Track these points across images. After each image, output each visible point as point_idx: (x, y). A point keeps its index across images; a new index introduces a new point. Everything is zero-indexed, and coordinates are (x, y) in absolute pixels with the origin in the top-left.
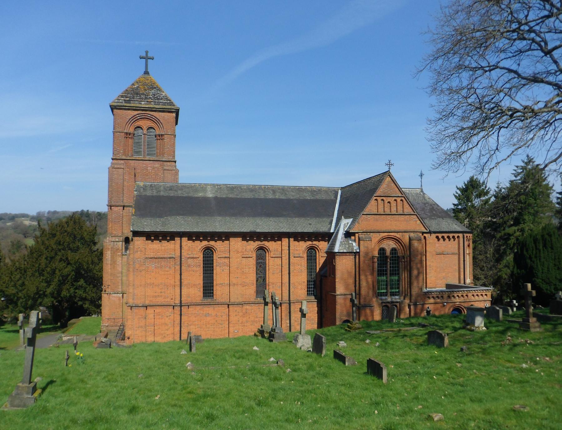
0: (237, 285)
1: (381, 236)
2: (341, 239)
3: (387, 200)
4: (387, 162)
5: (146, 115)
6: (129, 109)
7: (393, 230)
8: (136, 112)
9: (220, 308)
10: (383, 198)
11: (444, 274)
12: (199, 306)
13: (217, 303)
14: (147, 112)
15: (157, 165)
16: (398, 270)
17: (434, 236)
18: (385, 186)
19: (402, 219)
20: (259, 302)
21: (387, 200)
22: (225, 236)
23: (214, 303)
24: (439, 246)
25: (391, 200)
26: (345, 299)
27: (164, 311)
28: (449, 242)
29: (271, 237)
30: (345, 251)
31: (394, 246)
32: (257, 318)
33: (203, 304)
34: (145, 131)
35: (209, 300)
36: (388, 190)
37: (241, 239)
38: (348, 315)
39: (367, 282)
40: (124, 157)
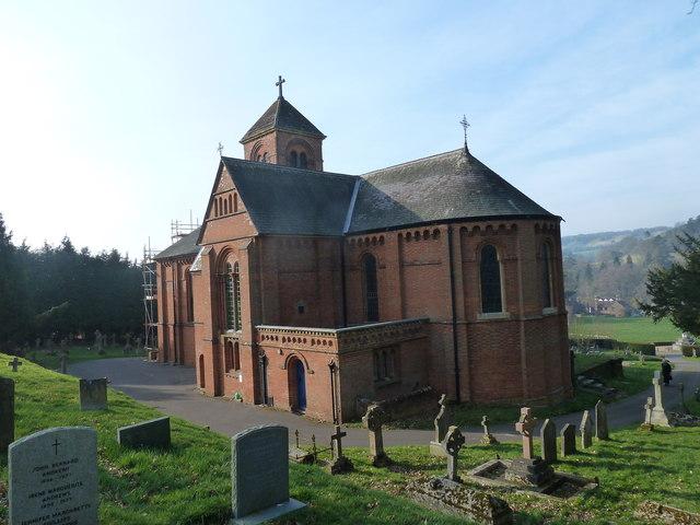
17: (396, 233)
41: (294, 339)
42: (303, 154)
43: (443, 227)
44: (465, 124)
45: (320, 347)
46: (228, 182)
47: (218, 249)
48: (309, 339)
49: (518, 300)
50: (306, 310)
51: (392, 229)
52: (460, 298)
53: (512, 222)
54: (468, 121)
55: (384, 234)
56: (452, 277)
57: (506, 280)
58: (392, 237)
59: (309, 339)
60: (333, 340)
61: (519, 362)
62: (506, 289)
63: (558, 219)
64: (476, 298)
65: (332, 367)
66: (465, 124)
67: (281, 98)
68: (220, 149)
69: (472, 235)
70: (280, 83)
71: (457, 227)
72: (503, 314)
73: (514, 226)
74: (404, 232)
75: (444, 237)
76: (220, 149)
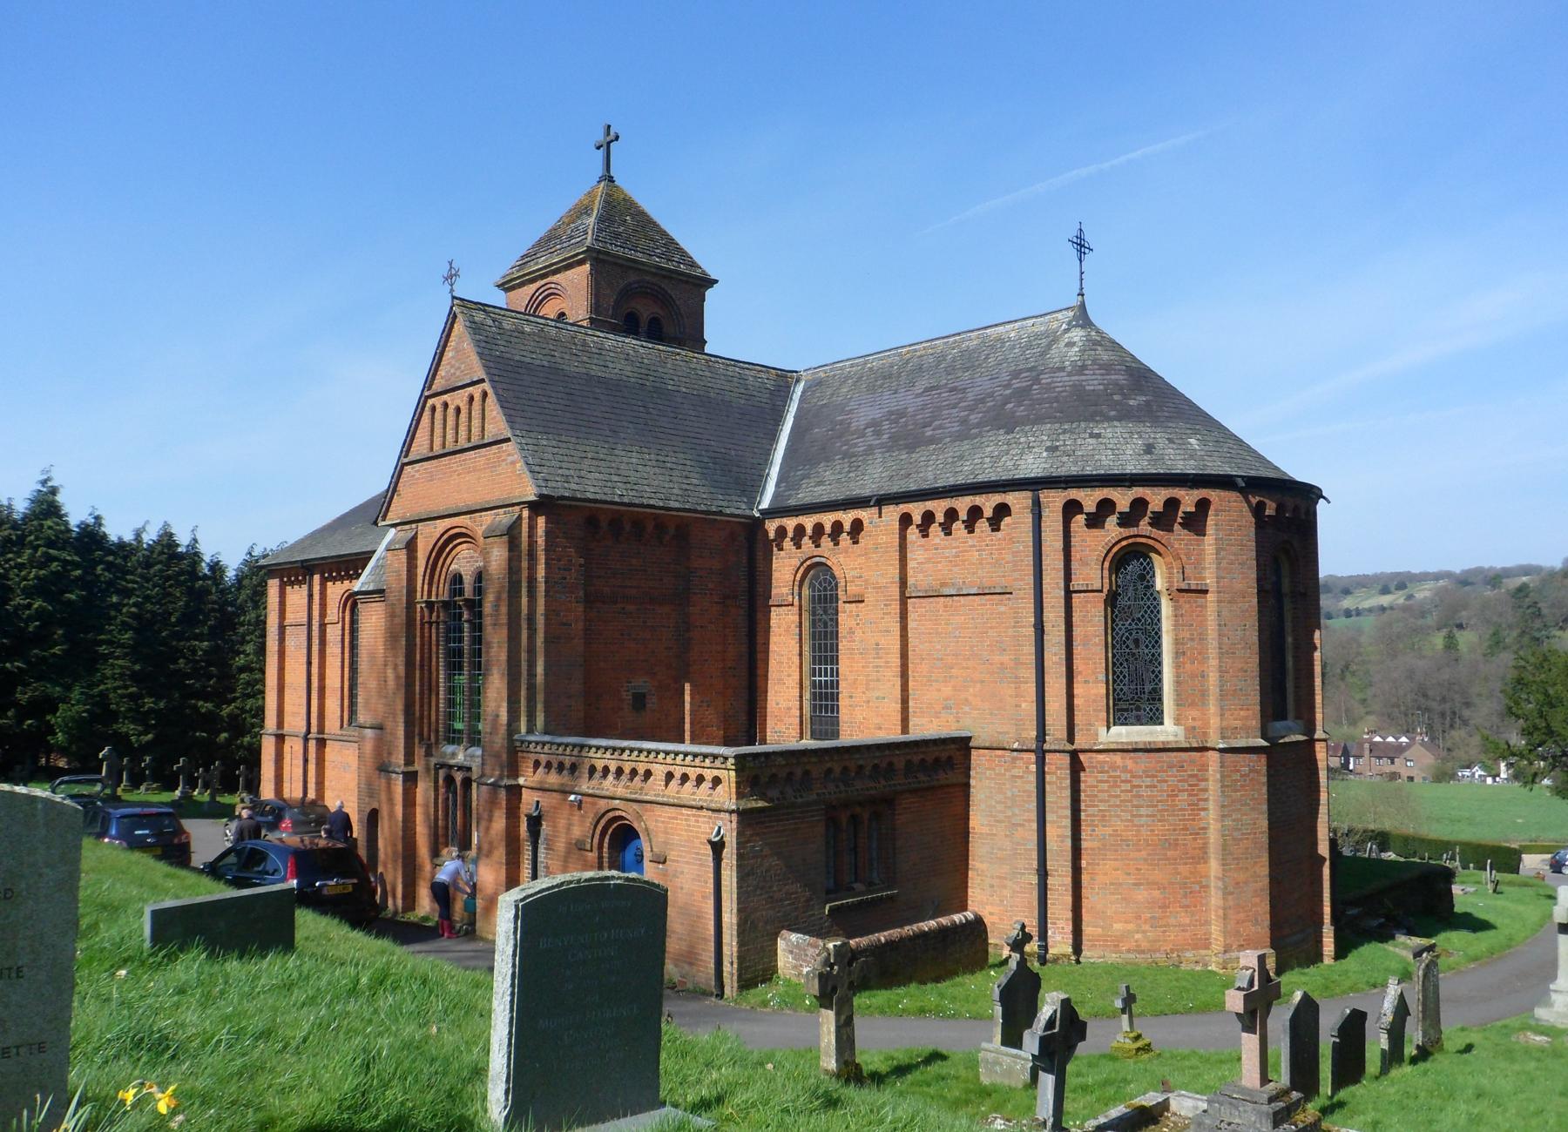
1: (441, 530)
5: (548, 286)
7: (462, 506)
8: (534, 287)
10: (445, 397)
17: (892, 513)
18: (450, 354)
19: (482, 461)
21: (453, 400)
24: (928, 560)
28: (971, 540)
41: (619, 771)
43: (1018, 501)
44: (1081, 246)
45: (688, 792)
46: (465, 360)
47: (429, 535)
48: (659, 771)
49: (1204, 694)
50: (652, 702)
51: (882, 501)
53: (1198, 494)
54: (1089, 238)
57: (1177, 642)
58: (882, 524)
59: (659, 771)
60: (722, 774)
61: (1202, 857)
62: (1177, 666)
63: (1308, 495)
64: (1093, 689)
65: (717, 847)
66: (1081, 246)
68: (451, 276)
69: (1095, 521)
71: (1054, 501)
72: (1168, 731)
73: (1203, 505)
74: (917, 510)
75: (1019, 522)
76: (451, 276)
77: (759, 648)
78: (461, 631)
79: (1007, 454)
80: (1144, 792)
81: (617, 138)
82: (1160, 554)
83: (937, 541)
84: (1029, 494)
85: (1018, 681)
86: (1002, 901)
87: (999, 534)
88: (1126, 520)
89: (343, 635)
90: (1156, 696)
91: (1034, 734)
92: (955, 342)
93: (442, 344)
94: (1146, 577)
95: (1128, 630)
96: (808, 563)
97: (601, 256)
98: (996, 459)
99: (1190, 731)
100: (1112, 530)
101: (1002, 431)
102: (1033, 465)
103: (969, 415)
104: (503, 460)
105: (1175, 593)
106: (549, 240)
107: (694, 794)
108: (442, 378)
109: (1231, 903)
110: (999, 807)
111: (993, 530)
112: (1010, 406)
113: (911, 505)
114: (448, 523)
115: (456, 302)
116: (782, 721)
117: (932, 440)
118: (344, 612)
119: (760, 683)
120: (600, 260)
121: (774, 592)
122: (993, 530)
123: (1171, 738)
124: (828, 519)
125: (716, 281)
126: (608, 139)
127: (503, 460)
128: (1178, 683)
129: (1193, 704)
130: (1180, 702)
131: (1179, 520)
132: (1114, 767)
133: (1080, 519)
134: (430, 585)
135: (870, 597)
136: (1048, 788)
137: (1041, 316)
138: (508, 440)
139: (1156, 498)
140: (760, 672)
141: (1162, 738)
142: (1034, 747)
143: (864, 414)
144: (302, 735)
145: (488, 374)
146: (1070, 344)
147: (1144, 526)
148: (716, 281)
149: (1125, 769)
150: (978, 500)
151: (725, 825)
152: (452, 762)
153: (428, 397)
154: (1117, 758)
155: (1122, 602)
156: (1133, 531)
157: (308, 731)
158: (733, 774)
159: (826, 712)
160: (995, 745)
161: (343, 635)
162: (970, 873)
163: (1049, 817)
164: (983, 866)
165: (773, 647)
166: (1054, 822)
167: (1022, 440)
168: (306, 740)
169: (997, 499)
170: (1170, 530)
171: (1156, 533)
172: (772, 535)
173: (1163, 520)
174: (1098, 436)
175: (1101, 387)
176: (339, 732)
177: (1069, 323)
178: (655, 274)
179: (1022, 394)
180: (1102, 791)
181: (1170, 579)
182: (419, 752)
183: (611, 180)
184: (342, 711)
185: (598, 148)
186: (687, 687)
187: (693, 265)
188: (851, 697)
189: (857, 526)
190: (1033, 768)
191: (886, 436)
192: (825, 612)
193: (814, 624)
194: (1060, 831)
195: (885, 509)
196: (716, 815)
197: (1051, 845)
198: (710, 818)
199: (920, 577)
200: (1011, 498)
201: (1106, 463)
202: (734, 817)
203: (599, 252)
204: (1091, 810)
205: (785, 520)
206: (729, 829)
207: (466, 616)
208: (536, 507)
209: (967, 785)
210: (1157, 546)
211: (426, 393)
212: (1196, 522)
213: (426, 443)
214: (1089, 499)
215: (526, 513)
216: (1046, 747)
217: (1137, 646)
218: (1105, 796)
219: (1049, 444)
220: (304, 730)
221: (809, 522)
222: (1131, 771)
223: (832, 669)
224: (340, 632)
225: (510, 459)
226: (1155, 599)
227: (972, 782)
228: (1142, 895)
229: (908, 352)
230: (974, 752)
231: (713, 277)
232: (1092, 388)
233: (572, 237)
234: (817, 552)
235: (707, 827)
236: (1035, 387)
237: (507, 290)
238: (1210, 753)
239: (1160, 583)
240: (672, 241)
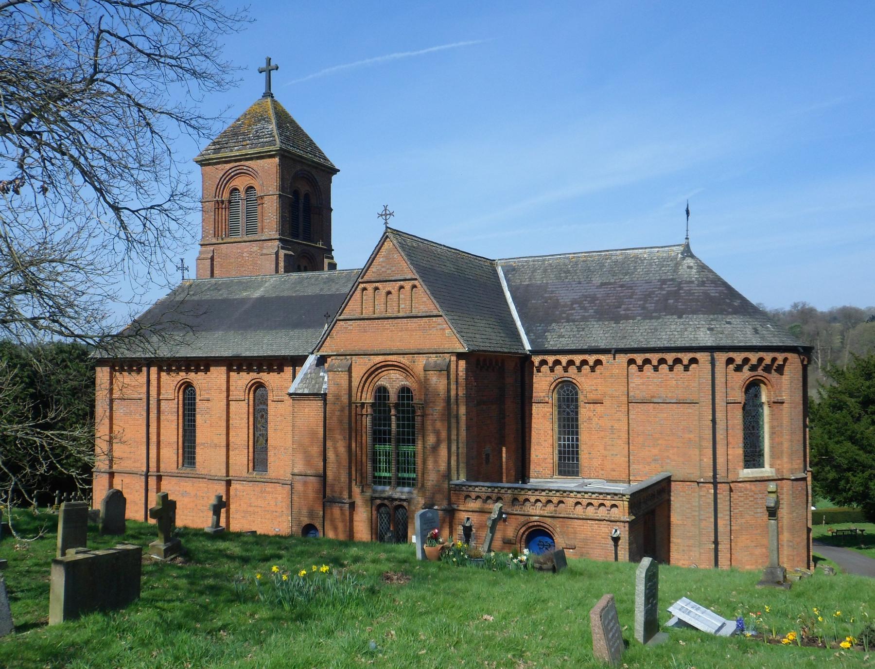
0: (220, 447)
2: (309, 368)
3: (384, 288)
4: (381, 210)
5: (241, 167)
6: (218, 163)
7: (394, 349)
8: (228, 166)
9: (201, 485)
10: (377, 284)
11: (655, 451)
12: (174, 478)
13: (197, 476)
14: (242, 163)
15: (255, 249)
16: (413, 435)
17: (623, 359)
18: (381, 259)
19: (414, 325)
20: (254, 479)
22: (203, 364)
23: (193, 476)
24: (643, 384)
25: (393, 287)
26: (305, 484)
27: (134, 482)
29: (176, 367)
30: (306, 391)
31: (405, 383)
32: (251, 506)
33: (179, 475)
34: (243, 196)
35: (188, 470)
36: (388, 267)
37: (225, 368)
38: (311, 514)
39: (337, 455)
40: (214, 241)
42: (307, 196)
43: (702, 357)
49: (782, 452)
52: (720, 450)
55: (602, 357)
56: (714, 421)
57: (772, 428)
62: (772, 438)
64: (737, 451)
65: (616, 540)
67: (268, 94)
69: (739, 369)
70: (268, 70)
72: (767, 471)
77: (527, 426)
78: (390, 420)
79: (686, 331)
80: (759, 501)
81: (277, 68)
82: (765, 384)
83: (649, 374)
84: (709, 354)
85: (701, 448)
86: (689, 558)
87: (688, 373)
88: (753, 368)
89: (178, 408)
90: (761, 454)
91: (711, 474)
92: (606, 255)
93: (375, 253)
94: (757, 396)
95: (750, 422)
96: (560, 380)
97: (286, 154)
98: (681, 333)
99: (778, 470)
100: (746, 373)
101: (675, 317)
102: (705, 338)
103: (643, 304)
104: (434, 327)
105: (772, 404)
106: (236, 134)
107: (597, 513)
108: (373, 272)
109: (795, 553)
110: (688, 511)
111: (685, 371)
112: (671, 301)
113: (635, 355)
114: (380, 358)
115: (389, 230)
116: (540, 465)
117: (627, 318)
118: (178, 393)
119: (527, 446)
120: (285, 156)
121: (534, 395)
122: (685, 371)
123: (770, 475)
124: (578, 358)
125: (339, 171)
126: (270, 68)
127: (434, 327)
128: (772, 447)
129: (778, 458)
130: (773, 456)
131: (774, 368)
132: (746, 489)
133: (731, 367)
134: (362, 393)
135: (607, 402)
136: (719, 501)
137: (662, 247)
138: (441, 316)
139: (768, 357)
140: (527, 439)
141: (766, 475)
142: (712, 481)
143: (565, 297)
144: (144, 473)
145: (420, 276)
146: (690, 267)
147: (760, 371)
148: (339, 171)
149: (751, 491)
150: (679, 355)
151: (620, 528)
152: (383, 495)
153: (360, 283)
154: (748, 485)
155: (748, 408)
156: (755, 373)
157: (148, 471)
158: (627, 503)
159: (569, 460)
160: (686, 480)
161: (178, 408)
162: (672, 545)
163: (719, 515)
164: (679, 541)
165: (533, 425)
166: (721, 518)
167: (691, 323)
168: (147, 477)
169: (691, 355)
170: (770, 372)
171: (765, 374)
172: (536, 364)
173: (768, 369)
174: (729, 323)
175: (717, 294)
176: (176, 471)
177: (682, 253)
178: (309, 166)
179: (676, 294)
180: (741, 501)
181: (769, 396)
182: (356, 490)
183: (272, 96)
184: (178, 457)
185: (261, 72)
186: (504, 449)
187: (326, 159)
188: (590, 453)
189: (598, 362)
190: (712, 491)
191: (592, 311)
192: (568, 407)
193: (559, 413)
194: (725, 522)
195: (617, 356)
196: (614, 524)
197: (720, 529)
198: (609, 525)
199: (638, 392)
200: (698, 355)
201: (740, 340)
202: (627, 525)
203: (285, 151)
204: (737, 511)
205: (546, 356)
206: (623, 532)
207: (393, 412)
208: (460, 356)
209: (669, 501)
210: (765, 380)
211: (360, 280)
212: (780, 370)
213: (359, 310)
214: (739, 357)
215: (454, 358)
216: (718, 480)
217: (754, 430)
218: (742, 504)
219: (707, 326)
220: (145, 469)
221: (564, 359)
222: (753, 491)
223: (573, 438)
224: (176, 406)
225: (440, 327)
226: (761, 405)
227: (672, 498)
228: (758, 551)
229: (574, 257)
230: (673, 483)
231: (337, 167)
232: (713, 295)
233: (259, 137)
234: (566, 374)
235: (606, 531)
236: (681, 291)
237: (202, 165)
238: (784, 481)
239: (764, 398)
240: (312, 143)
